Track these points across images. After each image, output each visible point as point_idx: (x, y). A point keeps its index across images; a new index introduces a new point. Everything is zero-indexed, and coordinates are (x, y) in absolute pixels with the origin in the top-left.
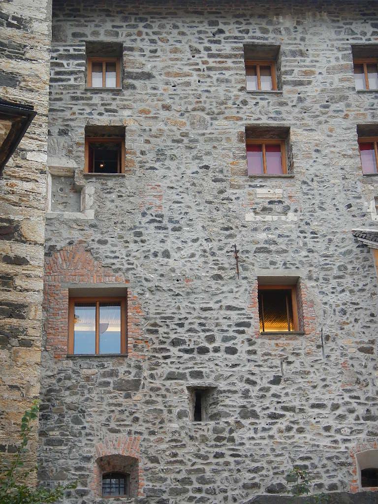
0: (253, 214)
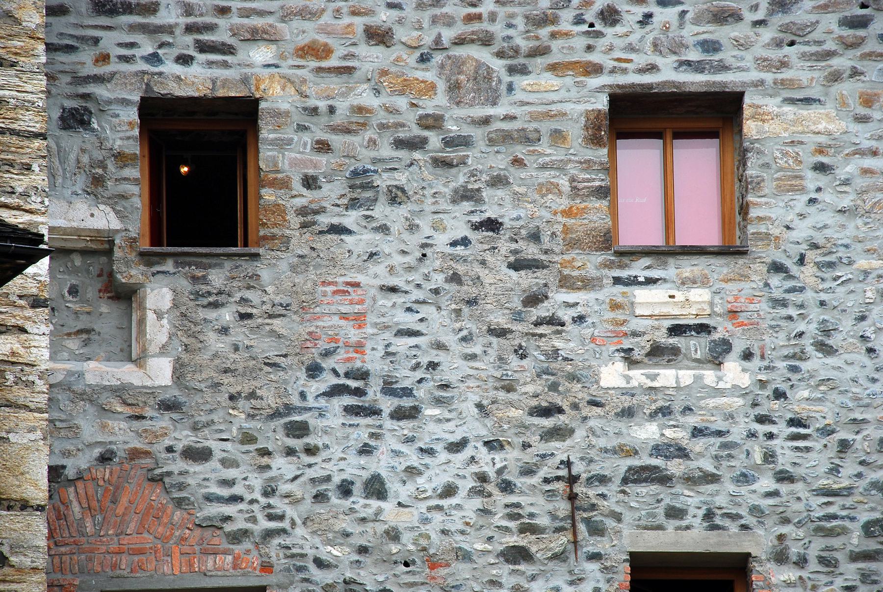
0: (620, 366)
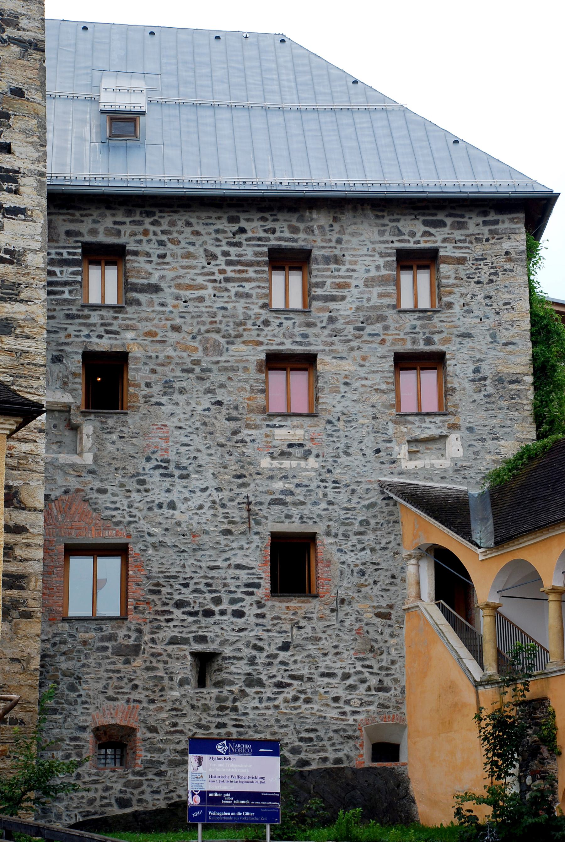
0: (269, 459)
